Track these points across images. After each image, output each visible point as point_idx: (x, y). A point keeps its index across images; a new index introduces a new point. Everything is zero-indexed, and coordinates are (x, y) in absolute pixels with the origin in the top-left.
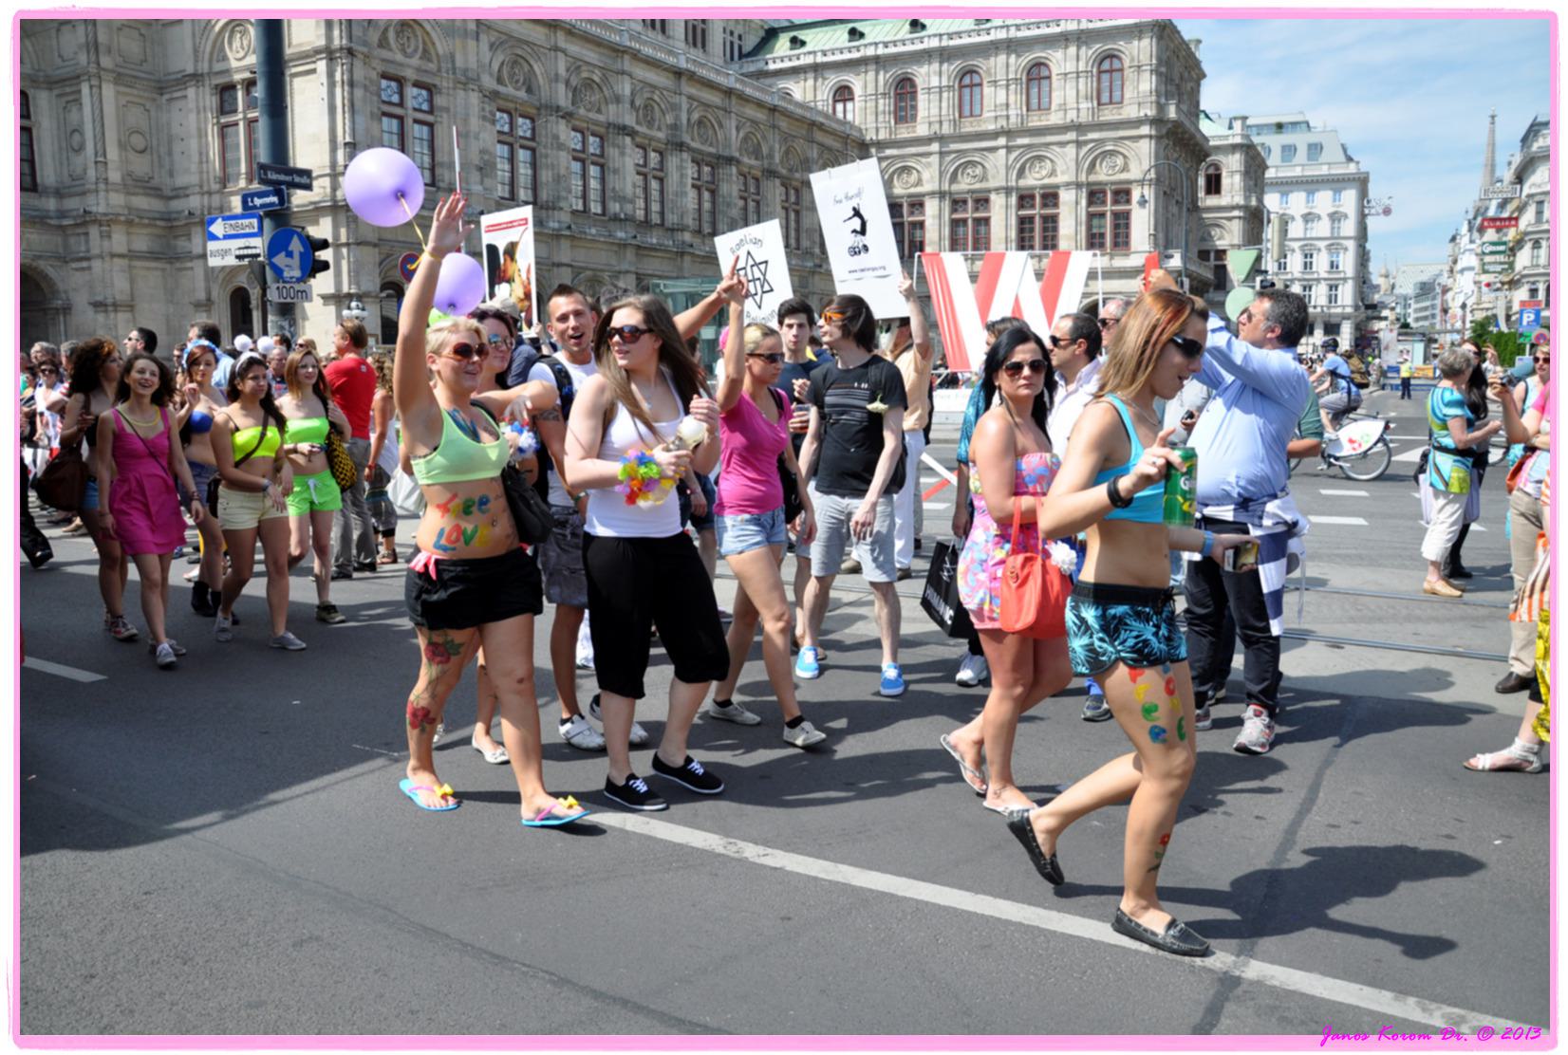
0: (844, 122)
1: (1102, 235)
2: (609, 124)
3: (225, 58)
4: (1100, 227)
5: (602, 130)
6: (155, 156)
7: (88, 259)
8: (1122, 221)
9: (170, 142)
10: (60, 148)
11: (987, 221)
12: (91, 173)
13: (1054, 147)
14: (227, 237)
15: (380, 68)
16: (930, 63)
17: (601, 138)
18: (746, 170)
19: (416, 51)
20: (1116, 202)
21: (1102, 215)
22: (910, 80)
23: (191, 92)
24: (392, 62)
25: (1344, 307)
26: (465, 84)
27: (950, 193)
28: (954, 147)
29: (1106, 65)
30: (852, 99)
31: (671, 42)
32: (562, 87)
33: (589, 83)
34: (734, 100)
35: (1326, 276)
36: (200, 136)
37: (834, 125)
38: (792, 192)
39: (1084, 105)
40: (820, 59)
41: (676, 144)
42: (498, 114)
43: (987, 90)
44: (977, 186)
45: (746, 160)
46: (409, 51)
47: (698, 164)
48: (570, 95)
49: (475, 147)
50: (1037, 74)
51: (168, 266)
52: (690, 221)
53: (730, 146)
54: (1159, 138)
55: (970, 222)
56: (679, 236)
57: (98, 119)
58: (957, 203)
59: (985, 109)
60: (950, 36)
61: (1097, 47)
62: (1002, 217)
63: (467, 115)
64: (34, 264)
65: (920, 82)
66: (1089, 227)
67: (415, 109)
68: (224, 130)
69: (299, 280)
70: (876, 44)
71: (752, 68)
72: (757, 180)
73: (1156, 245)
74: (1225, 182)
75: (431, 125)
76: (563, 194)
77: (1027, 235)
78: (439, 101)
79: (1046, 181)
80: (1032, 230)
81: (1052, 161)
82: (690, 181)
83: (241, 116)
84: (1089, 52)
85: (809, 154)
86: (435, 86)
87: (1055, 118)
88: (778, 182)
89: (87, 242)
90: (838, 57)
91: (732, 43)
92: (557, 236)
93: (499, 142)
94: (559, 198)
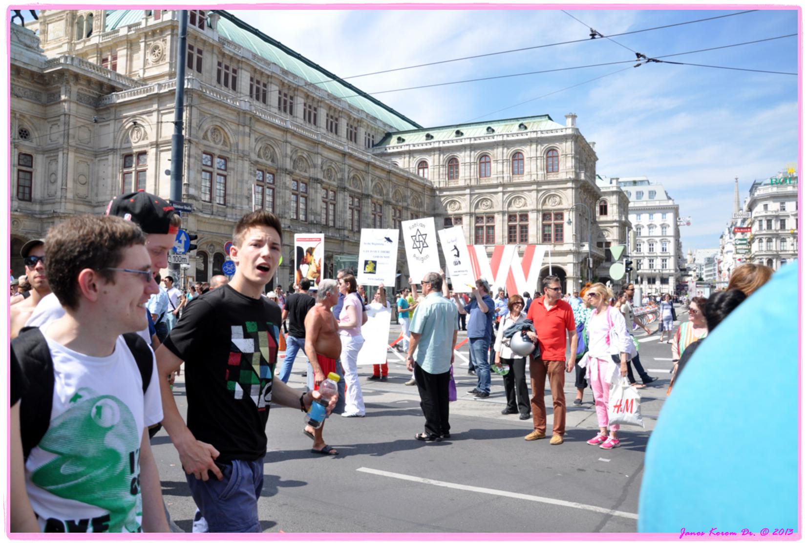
0: (423, 179)
1: (550, 235)
2: (310, 178)
3: (128, 142)
4: (549, 231)
5: (306, 181)
6: (90, 187)
8: (559, 228)
9: (98, 179)
10: (45, 181)
11: (493, 227)
12: (59, 194)
13: (525, 192)
15: (203, 149)
16: (465, 151)
17: (306, 184)
18: (375, 201)
19: (220, 141)
20: (556, 219)
21: (550, 225)
22: (455, 159)
23: (110, 157)
24: (209, 146)
25: (670, 270)
26: (242, 157)
27: (475, 214)
28: (477, 191)
29: (550, 154)
30: (427, 167)
31: (340, 138)
32: (288, 160)
33: (301, 158)
34: (370, 166)
35: (660, 255)
36: (113, 178)
37: (418, 180)
38: (398, 212)
39: (540, 173)
40: (412, 148)
41: (342, 188)
42: (257, 172)
43: (493, 165)
44: (489, 210)
45: (375, 196)
46: (217, 141)
47: (352, 197)
48: (292, 163)
49: (246, 187)
50: (517, 157)
52: (348, 225)
53: (368, 189)
54: (576, 189)
55: (485, 228)
56: (342, 232)
57: (65, 168)
58: (478, 219)
59: (492, 174)
60: (475, 139)
61: (546, 146)
62: (500, 226)
64: (26, 236)
65: (460, 160)
66: (543, 231)
67: (218, 169)
68: (124, 174)
69: (184, 253)
70: (439, 142)
71: (378, 151)
72: (381, 206)
73: (576, 240)
74: (609, 209)
75: (225, 176)
76: (287, 211)
77: (513, 234)
78: (230, 165)
79: (522, 209)
80: (515, 232)
81: (525, 199)
82: (348, 206)
83: (134, 169)
84: (542, 148)
85: (406, 194)
86: (228, 158)
87: (526, 178)
88: (391, 207)
90: (421, 147)
91: (369, 140)
93: (257, 185)
94: (285, 213)
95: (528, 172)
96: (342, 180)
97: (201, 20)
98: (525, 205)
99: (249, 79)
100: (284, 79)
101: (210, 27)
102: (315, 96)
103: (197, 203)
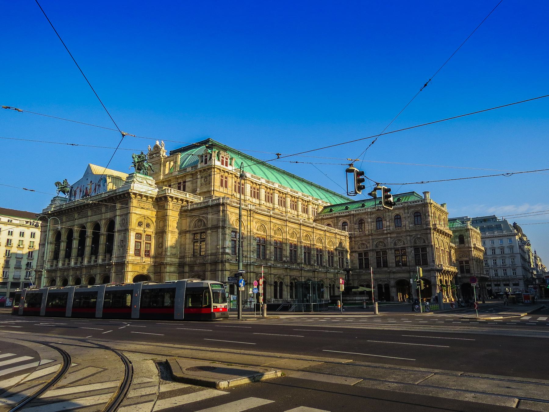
7: (160, 273)
14: (231, 280)
30: (347, 225)
33: (278, 229)
40: (338, 215)
44: (383, 248)
45: (318, 244)
51: (177, 274)
63: (250, 239)
65: (365, 220)
79: (402, 246)
89: (160, 269)
90: (343, 214)
92: (270, 267)
95: (404, 226)
96: (300, 237)
97: (226, 162)
98: (404, 244)
99: (250, 187)
100: (267, 185)
101: (231, 165)
102: (284, 192)
103: (229, 256)
